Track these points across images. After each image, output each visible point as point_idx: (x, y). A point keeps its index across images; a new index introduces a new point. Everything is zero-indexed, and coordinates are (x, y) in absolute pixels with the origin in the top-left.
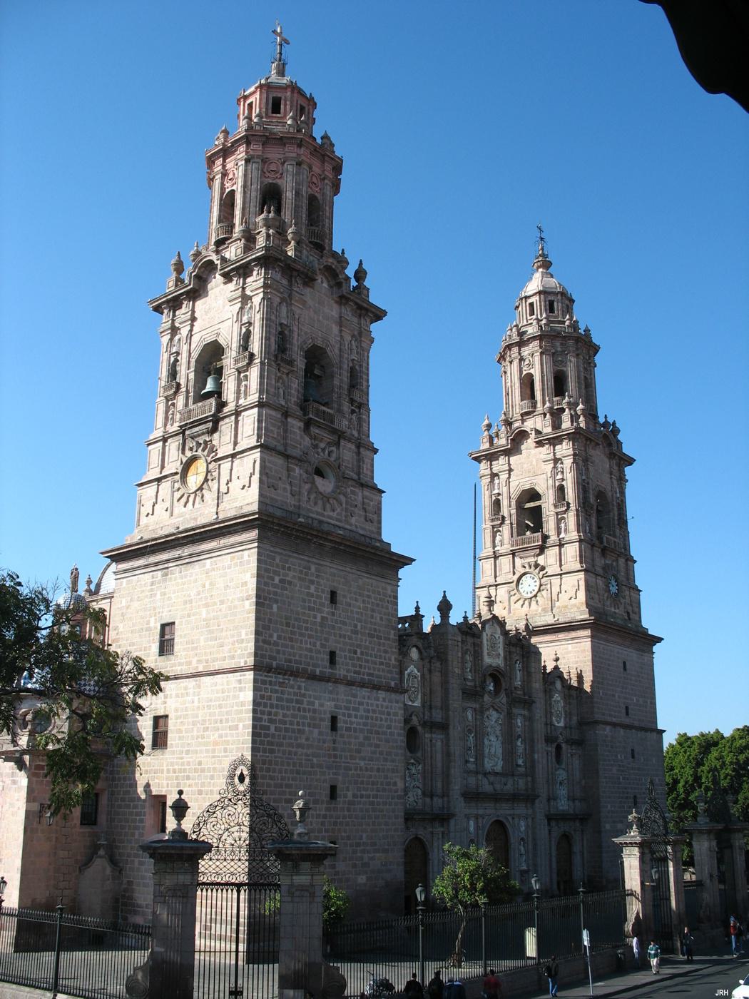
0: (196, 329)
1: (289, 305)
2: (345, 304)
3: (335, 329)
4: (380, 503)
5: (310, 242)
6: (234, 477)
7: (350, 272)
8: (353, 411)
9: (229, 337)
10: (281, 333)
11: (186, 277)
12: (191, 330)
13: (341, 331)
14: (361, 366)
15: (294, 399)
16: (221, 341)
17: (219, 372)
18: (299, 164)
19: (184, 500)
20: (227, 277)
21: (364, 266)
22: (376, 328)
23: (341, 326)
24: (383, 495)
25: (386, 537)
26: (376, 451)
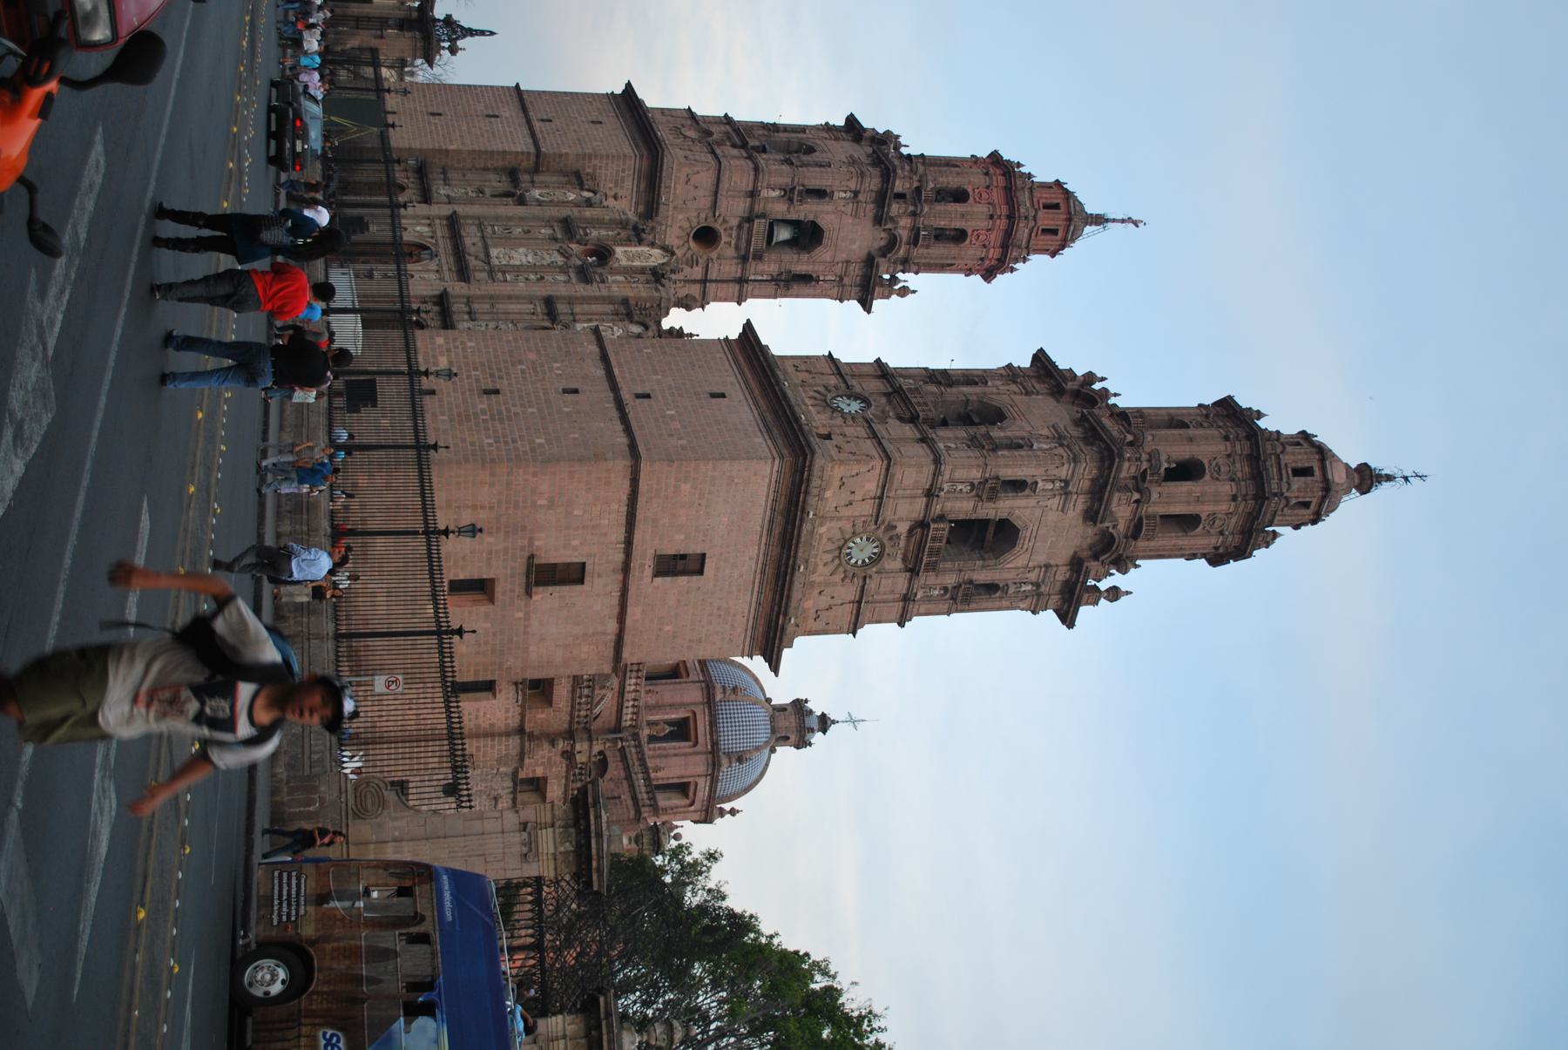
2: (1071, 569)
3: (1040, 558)
5: (1141, 519)
7: (1116, 579)
8: (946, 589)
9: (1012, 430)
12: (1015, 393)
13: (1041, 567)
14: (1001, 598)
15: (948, 505)
20: (1079, 422)
22: (1049, 617)
23: (1047, 566)
24: (851, 635)
25: (799, 641)
26: (901, 624)
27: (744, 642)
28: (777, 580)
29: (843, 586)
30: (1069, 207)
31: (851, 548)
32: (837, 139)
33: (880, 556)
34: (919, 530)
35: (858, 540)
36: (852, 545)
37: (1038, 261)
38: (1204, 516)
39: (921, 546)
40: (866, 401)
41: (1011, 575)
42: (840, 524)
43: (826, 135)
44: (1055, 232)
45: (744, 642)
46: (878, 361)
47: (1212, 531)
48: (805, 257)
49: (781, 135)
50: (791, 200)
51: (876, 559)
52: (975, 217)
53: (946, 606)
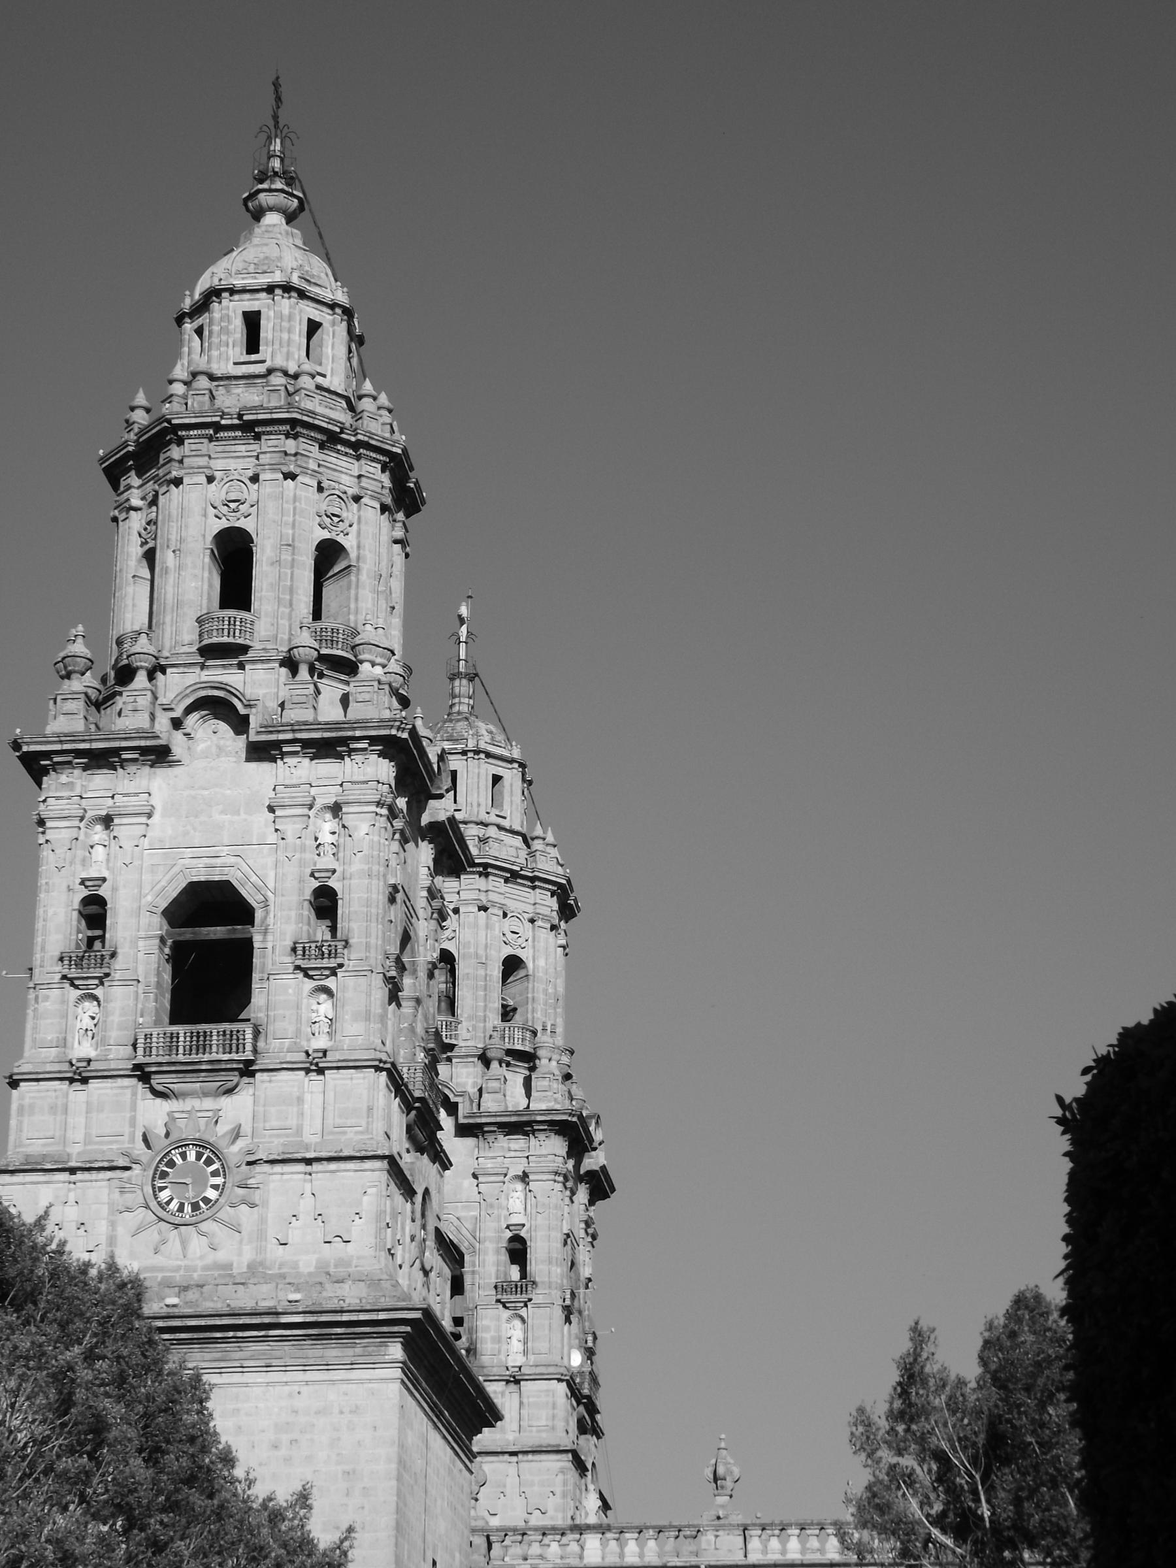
15: (114, 1035)
27: (361, 1381)
28: (215, 1341)
29: (265, 1203)
31: (181, 1209)
33: (201, 1145)
34: (156, 1081)
35: (164, 1196)
36: (174, 1206)
38: (224, 524)
39: (190, 1070)
41: (291, 871)
42: (120, 1230)
45: (361, 1381)
47: (253, 498)
53: (351, 982)
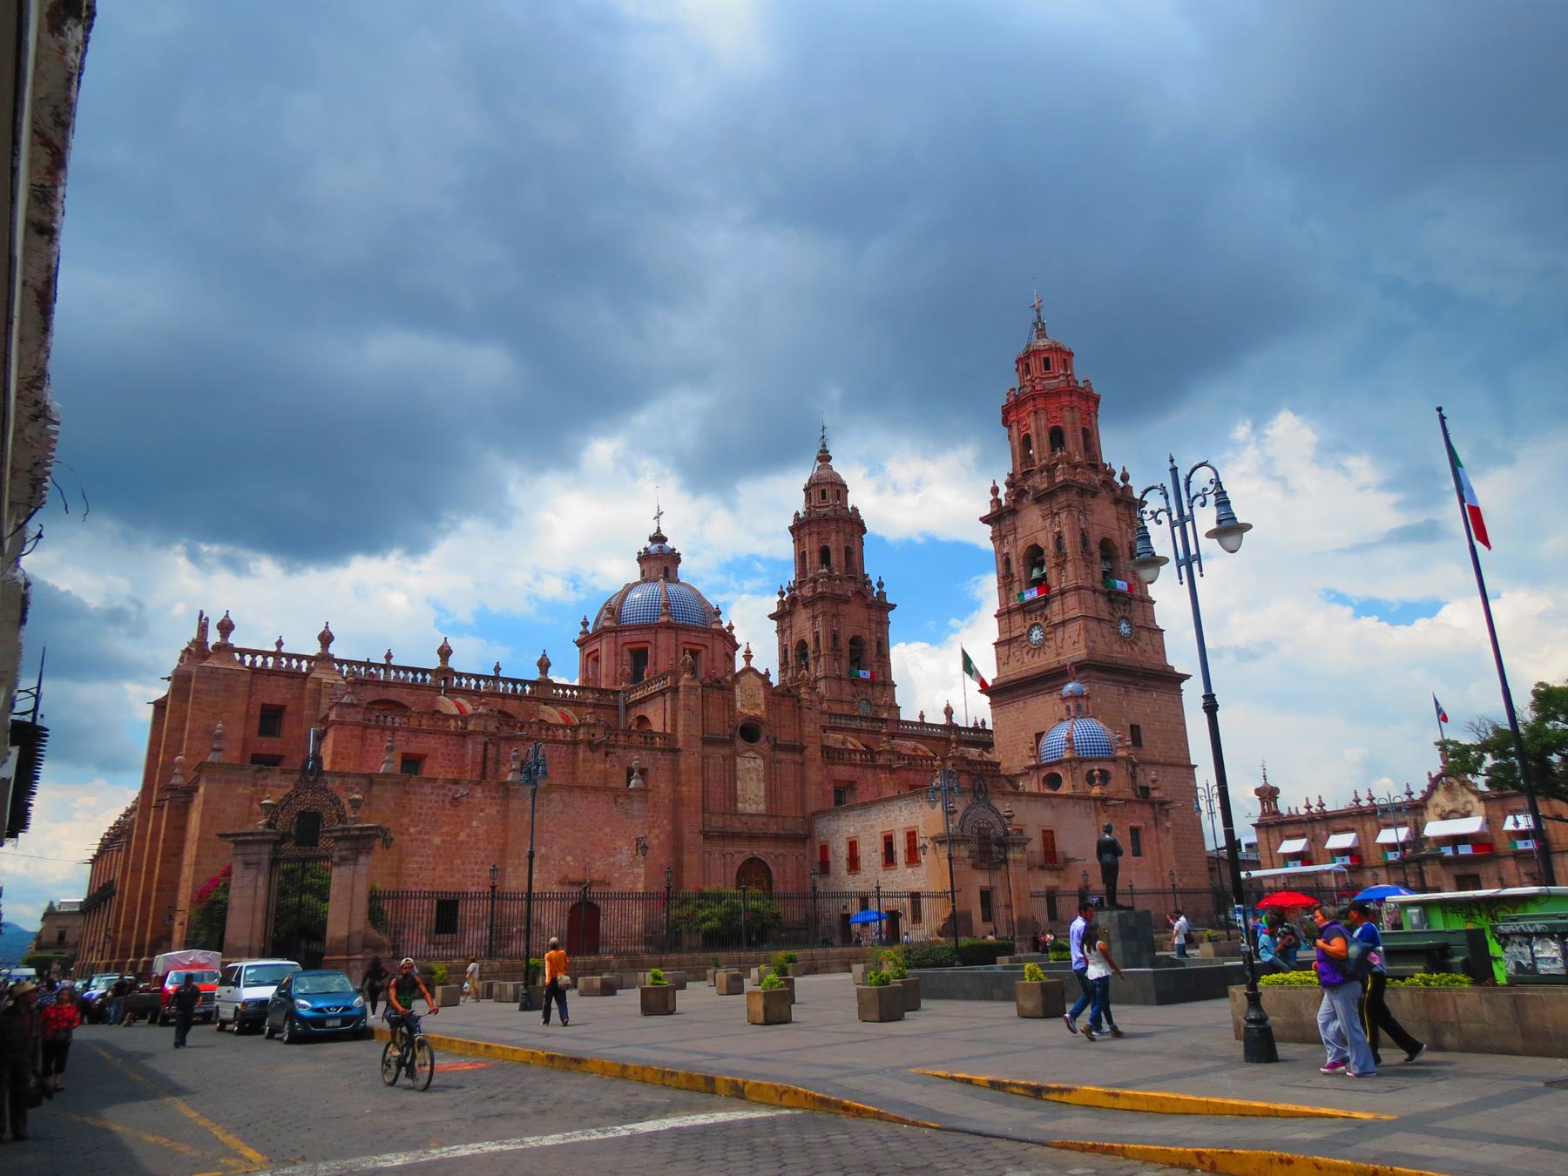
0: (1019, 536)
1: (1085, 515)
4: (1162, 639)
5: (1089, 464)
6: (1066, 636)
7: (1117, 478)
9: (1046, 540)
10: (1083, 535)
11: (1001, 496)
16: (1041, 544)
17: (1041, 564)
18: (1073, 408)
19: (1031, 653)
21: (1127, 470)
23: (1118, 519)
25: (1170, 662)
26: (1154, 602)
30: (821, 484)
32: (791, 626)
37: (853, 500)
40: (1033, 626)
43: (788, 632)
44: (838, 491)
46: (996, 616)
48: (868, 647)
49: (789, 660)
50: (841, 656)
51: (1129, 621)
52: (835, 543)
